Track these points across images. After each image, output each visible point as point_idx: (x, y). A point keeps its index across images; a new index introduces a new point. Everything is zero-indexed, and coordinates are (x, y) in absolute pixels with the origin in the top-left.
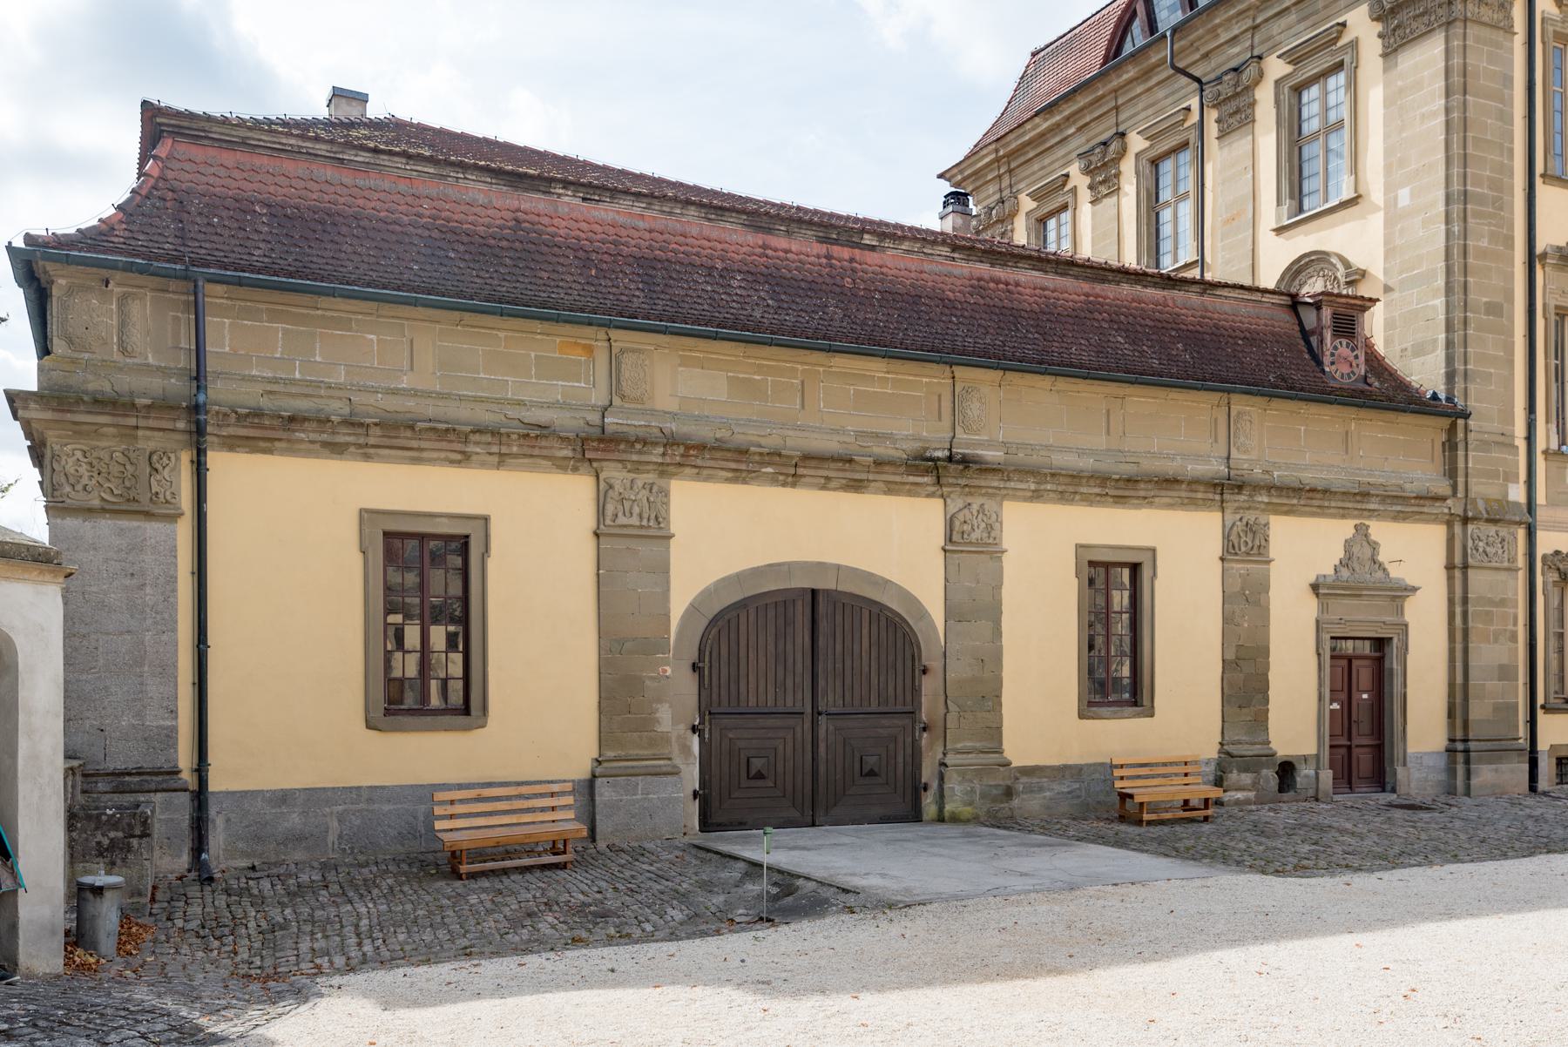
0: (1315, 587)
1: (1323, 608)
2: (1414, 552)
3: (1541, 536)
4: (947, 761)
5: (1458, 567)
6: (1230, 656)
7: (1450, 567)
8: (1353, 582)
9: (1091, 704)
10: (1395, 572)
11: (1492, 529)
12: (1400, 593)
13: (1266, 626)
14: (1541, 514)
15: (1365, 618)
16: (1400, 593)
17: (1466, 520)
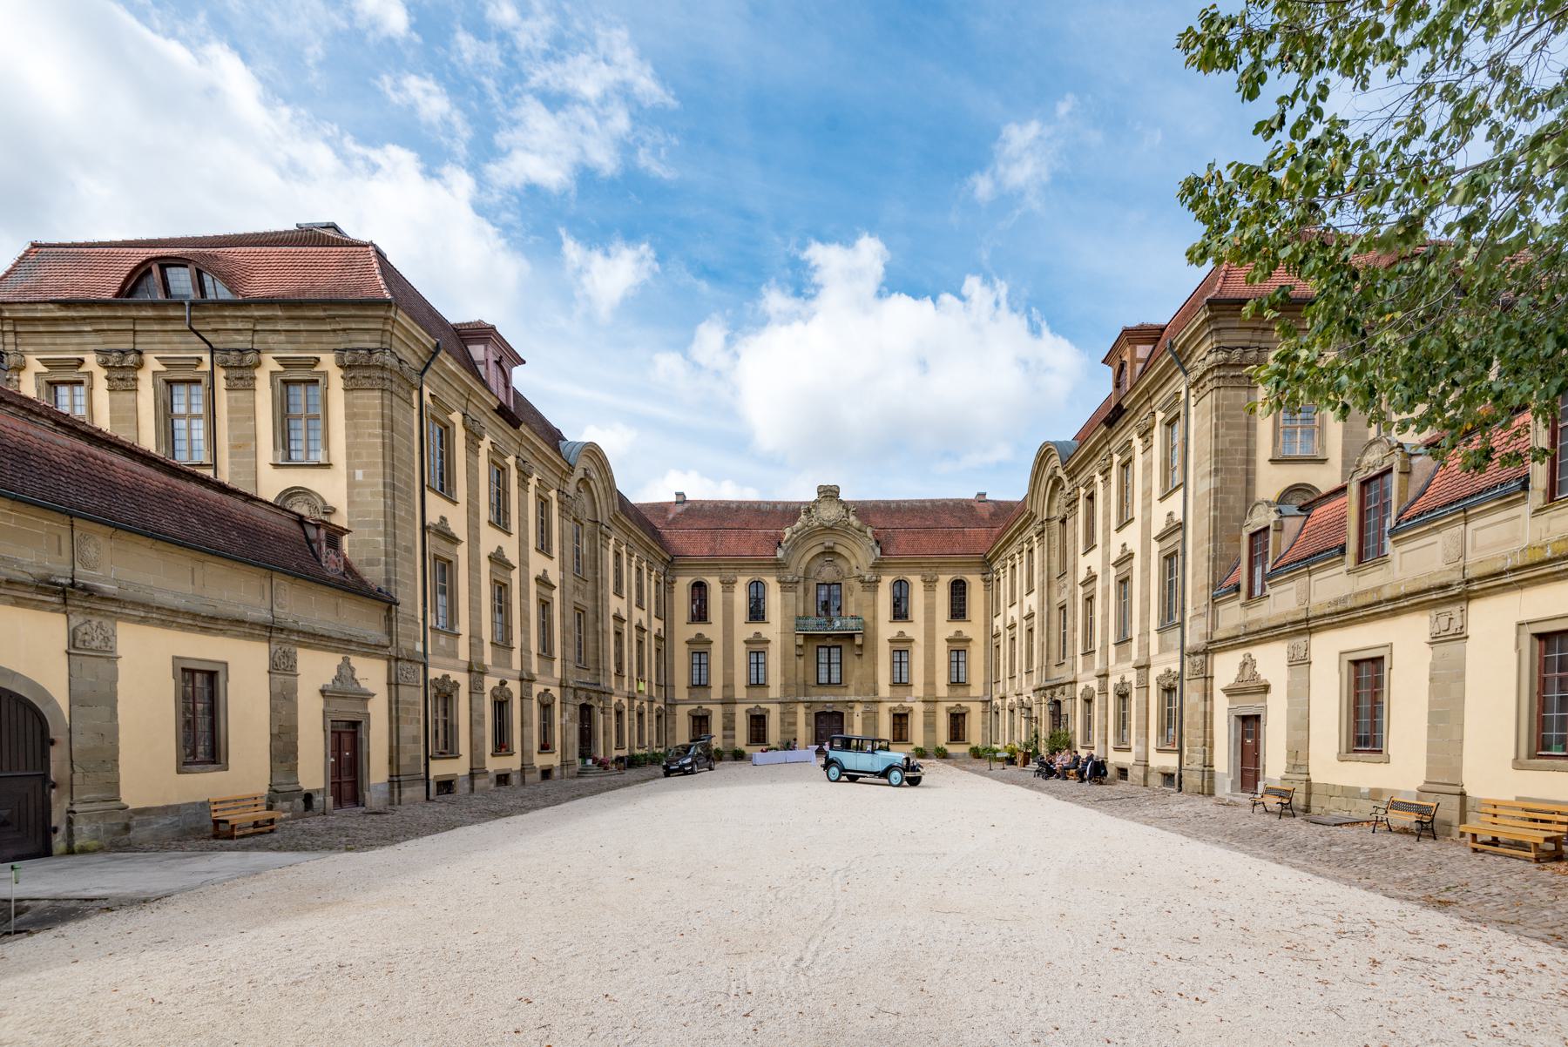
0: (323, 692)
1: (327, 704)
2: (371, 674)
3: (430, 669)
4: (75, 808)
5: (393, 684)
6: (275, 731)
7: (389, 684)
8: (341, 691)
9: (185, 763)
10: (363, 685)
11: (408, 665)
12: (366, 697)
13: (296, 714)
14: (430, 658)
15: (348, 711)
16: (366, 697)
17: (397, 659)
